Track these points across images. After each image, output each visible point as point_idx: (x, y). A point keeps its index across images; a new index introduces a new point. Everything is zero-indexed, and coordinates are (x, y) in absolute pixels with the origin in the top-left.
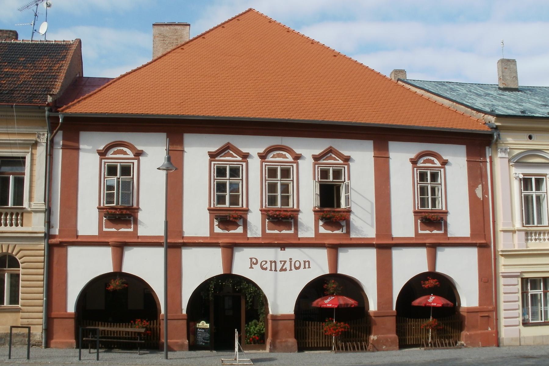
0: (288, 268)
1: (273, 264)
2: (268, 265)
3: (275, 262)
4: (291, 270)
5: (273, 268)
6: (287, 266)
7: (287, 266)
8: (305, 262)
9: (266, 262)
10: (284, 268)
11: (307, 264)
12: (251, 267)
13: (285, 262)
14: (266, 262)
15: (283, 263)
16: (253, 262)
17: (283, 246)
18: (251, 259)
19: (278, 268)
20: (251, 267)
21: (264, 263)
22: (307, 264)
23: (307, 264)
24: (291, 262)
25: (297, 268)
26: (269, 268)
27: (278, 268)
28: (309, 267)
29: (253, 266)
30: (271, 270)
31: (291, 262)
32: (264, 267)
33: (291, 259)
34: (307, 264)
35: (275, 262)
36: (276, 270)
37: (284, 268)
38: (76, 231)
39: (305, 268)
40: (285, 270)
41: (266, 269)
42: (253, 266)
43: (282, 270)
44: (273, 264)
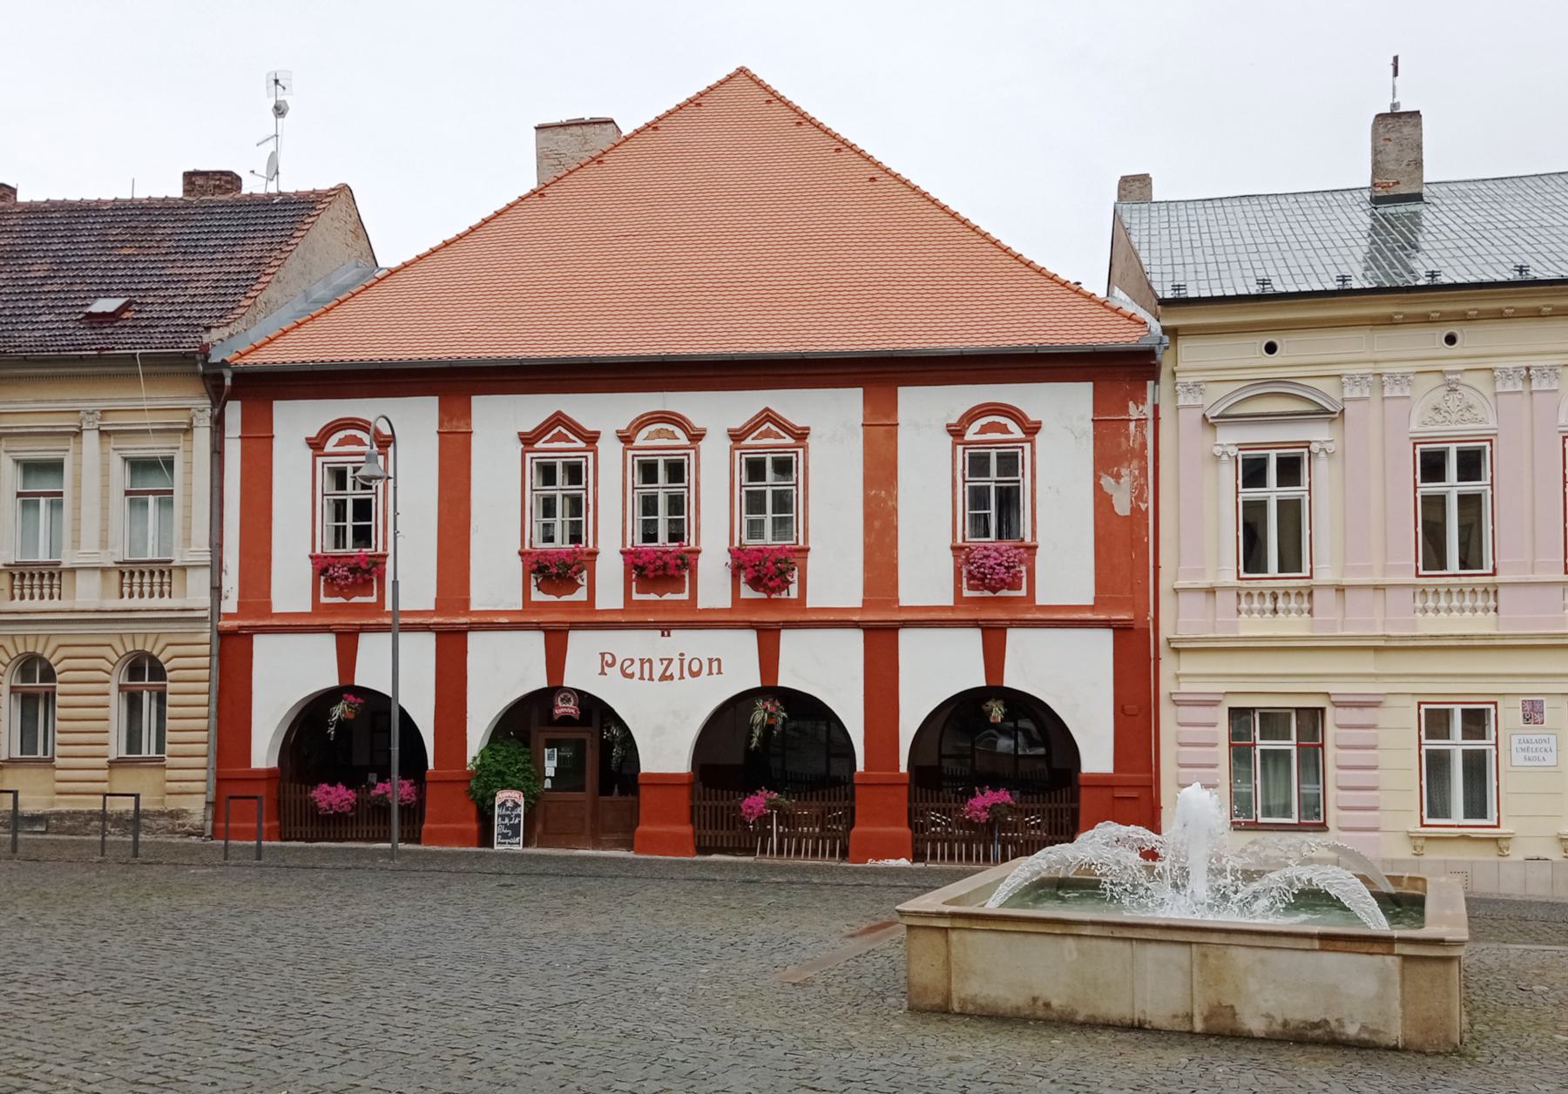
0: (677, 675)
1: (647, 666)
2: (636, 668)
3: (650, 661)
4: (682, 677)
5: (646, 675)
6: (674, 669)
7: (674, 669)
8: (711, 661)
9: (632, 661)
10: (668, 674)
11: (715, 665)
12: (603, 673)
13: (671, 660)
14: (632, 661)
15: (666, 663)
16: (607, 662)
17: (666, 628)
18: (603, 655)
19: (656, 676)
20: (603, 673)
21: (628, 663)
22: (715, 666)
23: (715, 665)
24: (682, 661)
25: (694, 674)
26: (638, 675)
27: (656, 676)
28: (719, 672)
29: (607, 669)
30: (642, 678)
31: (682, 661)
32: (629, 671)
33: (682, 655)
34: (715, 666)
35: (650, 661)
36: (651, 679)
37: (668, 674)
38: (269, 604)
39: (710, 673)
40: (671, 677)
41: (631, 676)
42: (607, 669)
43: (663, 678)
44: (647, 666)
